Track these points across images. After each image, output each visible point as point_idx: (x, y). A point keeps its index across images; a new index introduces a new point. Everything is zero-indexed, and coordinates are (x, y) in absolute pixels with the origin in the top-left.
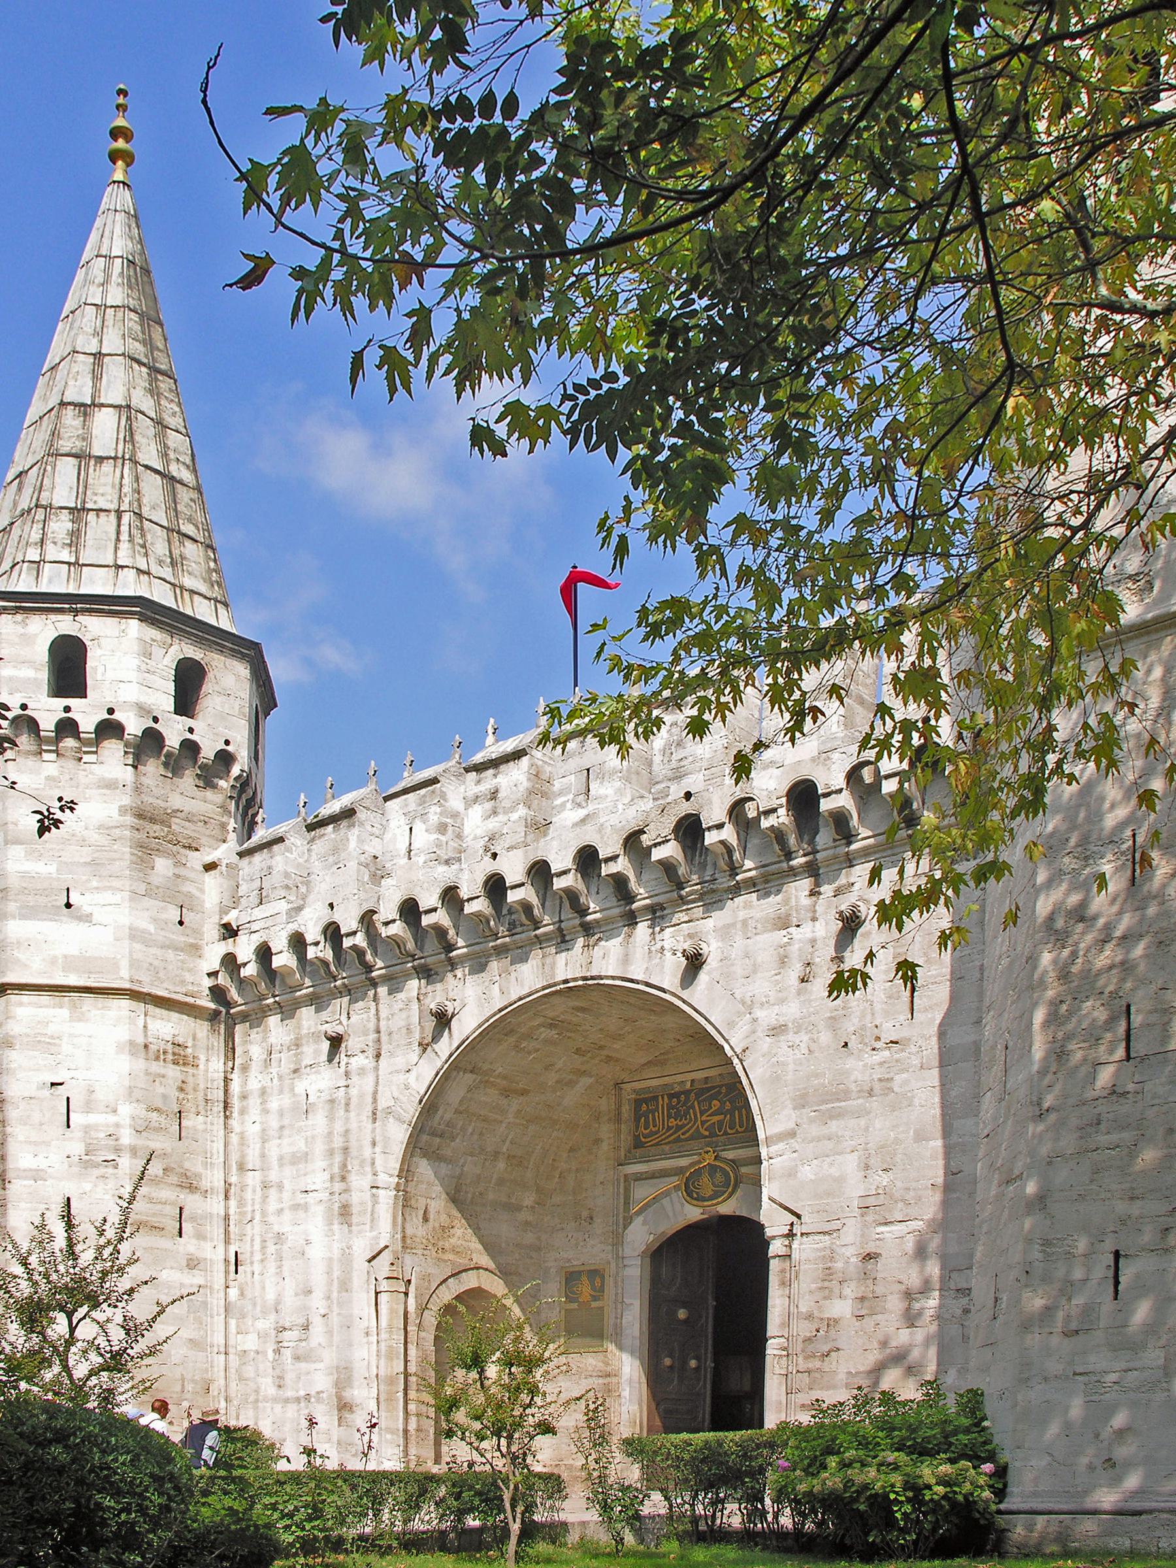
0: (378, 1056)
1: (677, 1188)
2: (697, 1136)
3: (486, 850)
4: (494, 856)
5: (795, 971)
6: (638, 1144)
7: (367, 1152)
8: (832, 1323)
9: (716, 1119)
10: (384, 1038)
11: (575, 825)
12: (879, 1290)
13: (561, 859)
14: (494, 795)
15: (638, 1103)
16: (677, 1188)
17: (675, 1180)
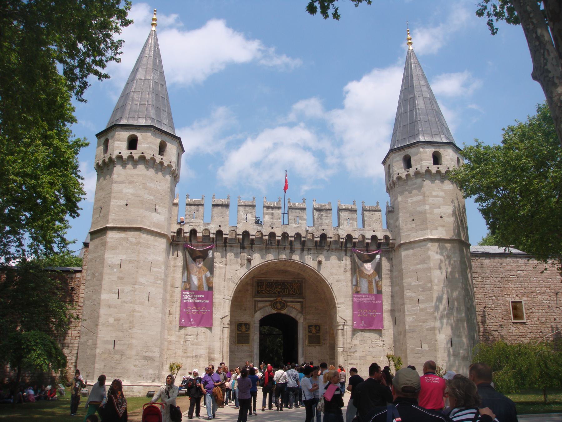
0: (226, 265)
1: (270, 305)
2: (275, 293)
3: (270, 226)
4: (272, 228)
5: (343, 269)
6: (258, 292)
7: (222, 289)
8: (355, 345)
9: (280, 290)
10: (228, 261)
11: (295, 227)
12: (365, 339)
13: (292, 234)
14: (272, 214)
15: (258, 283)
16: (270, 305)
17: (269, 303)
